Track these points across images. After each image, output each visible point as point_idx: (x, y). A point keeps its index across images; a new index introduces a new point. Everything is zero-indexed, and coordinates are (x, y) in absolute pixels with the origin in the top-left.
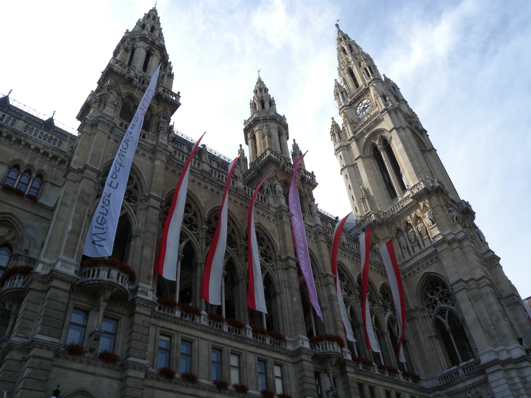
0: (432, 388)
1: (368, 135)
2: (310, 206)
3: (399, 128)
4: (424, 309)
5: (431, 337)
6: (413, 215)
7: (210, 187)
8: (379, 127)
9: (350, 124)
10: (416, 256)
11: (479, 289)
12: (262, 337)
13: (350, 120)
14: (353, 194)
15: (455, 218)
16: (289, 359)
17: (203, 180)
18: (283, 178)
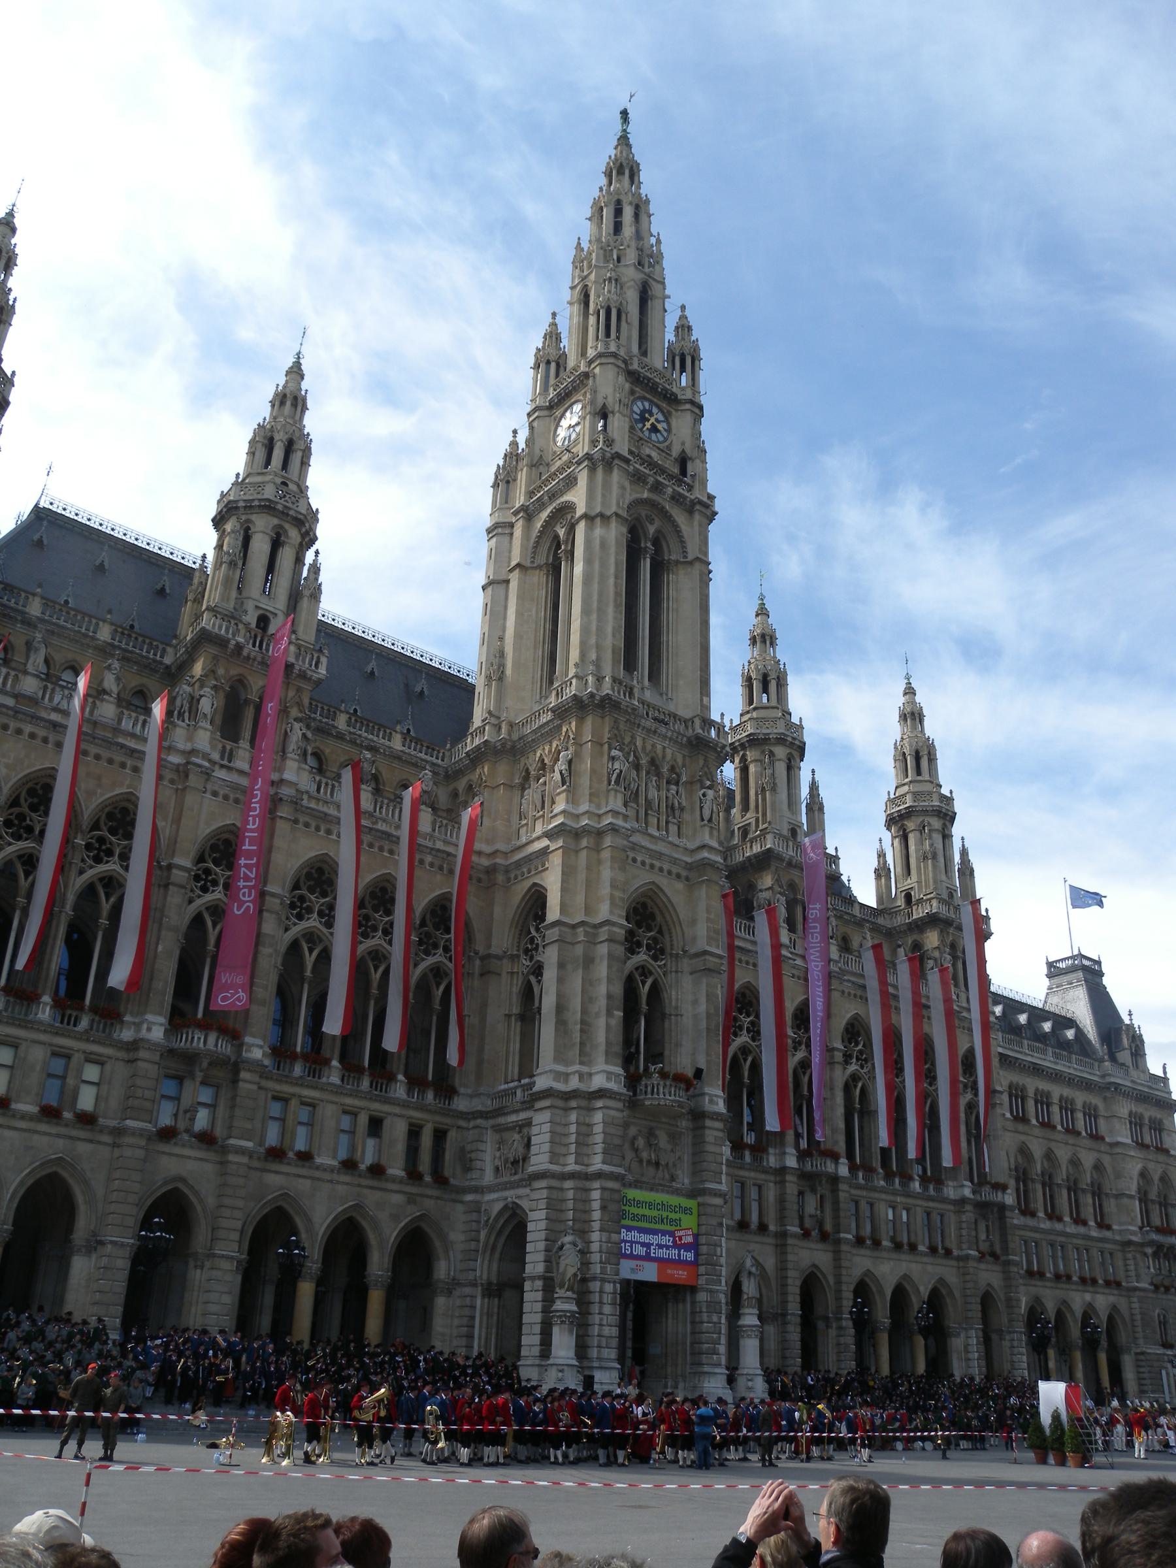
0: (473, 1113)
1: (549, 510)
2: (286, 732)
3: (597, 516)
4: (518, 956)
5: (509, 1016)
6: (554, 745)
7: (28, 728)
8: (568, 497)
9: (532, 466)
10: (533, 841)
11: (595, 944)
12: (74, 1014)
13: (537, 452)
14: (484, 660)
15: (615, 775)
16: (121, 1054)
17: (14, 717)
18: (234, 671)
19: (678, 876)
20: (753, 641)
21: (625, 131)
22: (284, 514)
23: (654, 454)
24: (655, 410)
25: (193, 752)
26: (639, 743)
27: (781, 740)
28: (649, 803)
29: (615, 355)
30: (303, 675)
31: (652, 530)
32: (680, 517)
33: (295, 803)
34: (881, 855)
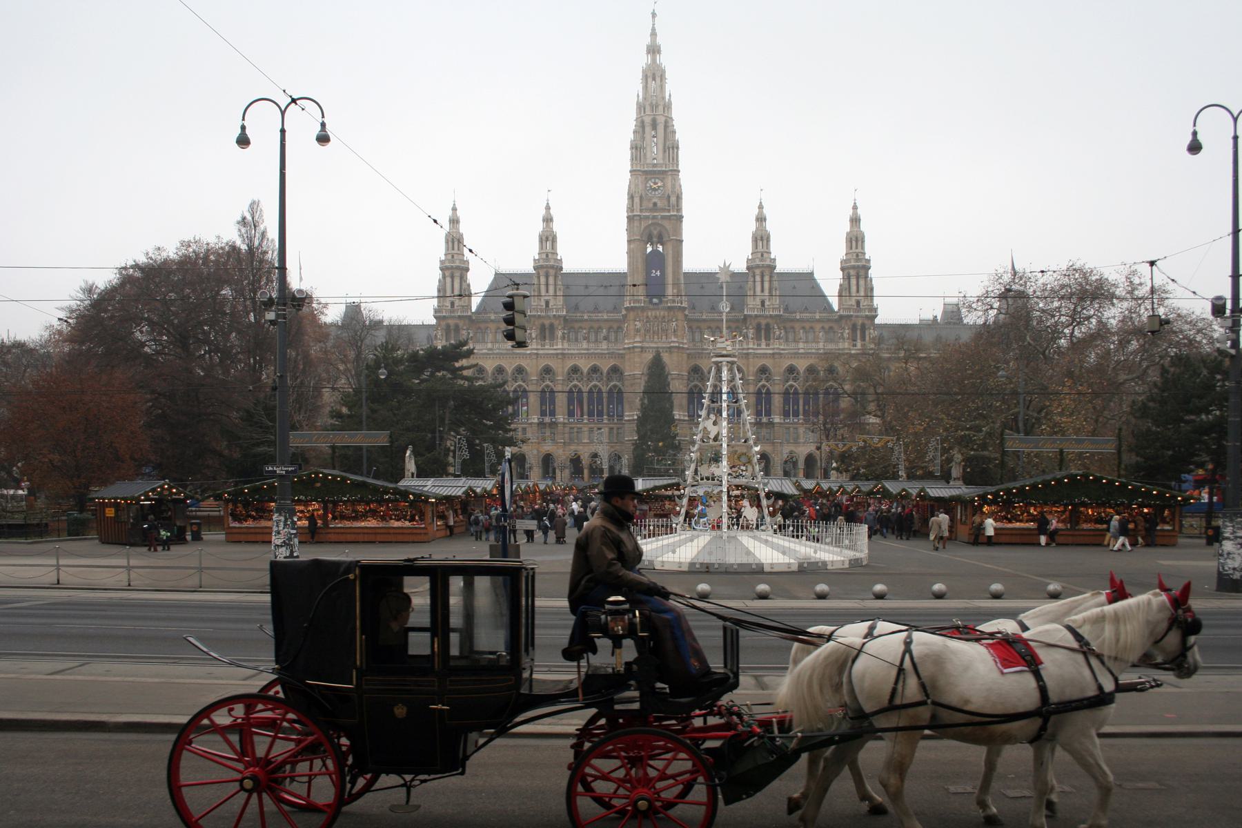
18: (541, 321)
20: (757, 219)
22: (547, 267)
27: (758, 267)
31: (655, 232)
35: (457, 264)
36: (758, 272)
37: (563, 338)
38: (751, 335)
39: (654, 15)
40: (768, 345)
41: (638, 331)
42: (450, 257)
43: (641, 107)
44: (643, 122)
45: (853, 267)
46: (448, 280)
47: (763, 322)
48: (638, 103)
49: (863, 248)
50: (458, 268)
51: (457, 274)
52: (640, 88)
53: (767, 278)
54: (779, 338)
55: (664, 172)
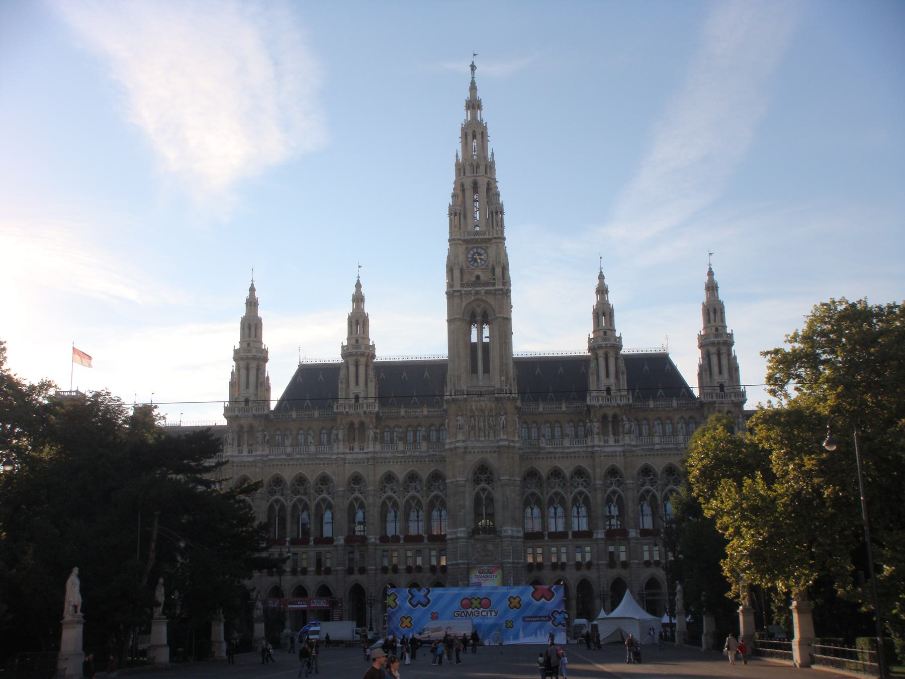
19: (495, 452)
21: (473, 78)
22: (356, 354)
23: (479, 273)
24: (479, 250)
25: (338, 454)
26: (474, 408)
27: (600, 347)
28: (480, 429)
29: (454, 240)
30: (370, 413)
31: (479, 310)
32: (490, 300)
33: (374, 458)
34: (700, 366)
35: (254, 353)
36: (601, 353)
37: (376, 439)
38: (596, 430)
39: (473, 67)
40: (616, 441)
41: (461, 428)
42: (245, 345)
43: (460, 169)
44: (463, 185)
45: (713, 344)
46: (243, 372)
47: (610, 413)
48: (457, 164)
49: (723, 320)
50: (254, 358)
51: (253, 365)
52: (459, 147)
53: (612, 361)
54: (629, 432)
55: (489, 240)
